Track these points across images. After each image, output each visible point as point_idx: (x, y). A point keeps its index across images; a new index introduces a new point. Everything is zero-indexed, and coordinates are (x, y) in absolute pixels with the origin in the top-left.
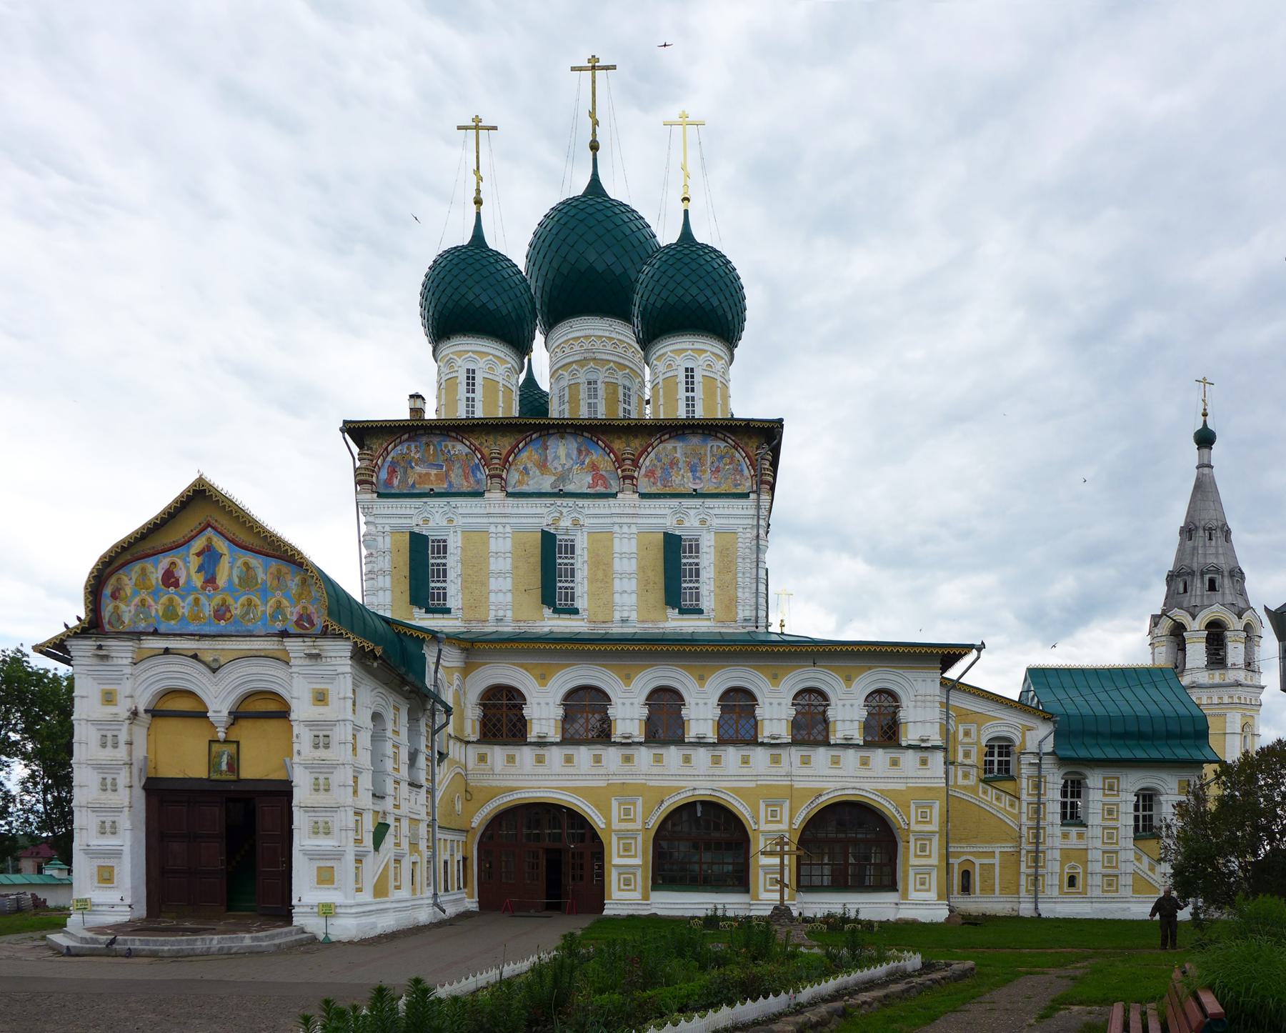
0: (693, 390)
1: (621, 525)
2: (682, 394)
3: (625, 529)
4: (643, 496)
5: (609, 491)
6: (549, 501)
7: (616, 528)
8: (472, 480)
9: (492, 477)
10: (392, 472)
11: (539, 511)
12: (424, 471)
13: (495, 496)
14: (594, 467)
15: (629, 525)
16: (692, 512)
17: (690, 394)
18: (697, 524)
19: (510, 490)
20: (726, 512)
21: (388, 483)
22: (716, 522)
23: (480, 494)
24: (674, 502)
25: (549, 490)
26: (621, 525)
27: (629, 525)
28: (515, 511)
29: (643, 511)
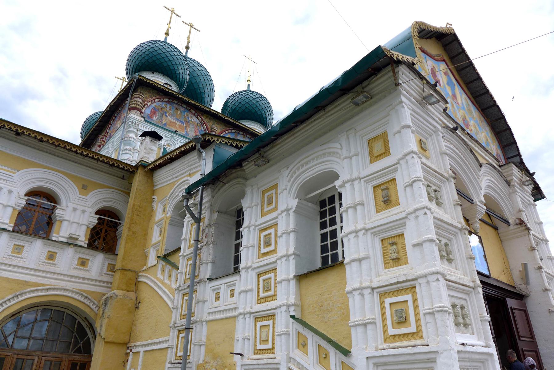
10: (154, 111)
12: (173, 121)
21: (150, 116)
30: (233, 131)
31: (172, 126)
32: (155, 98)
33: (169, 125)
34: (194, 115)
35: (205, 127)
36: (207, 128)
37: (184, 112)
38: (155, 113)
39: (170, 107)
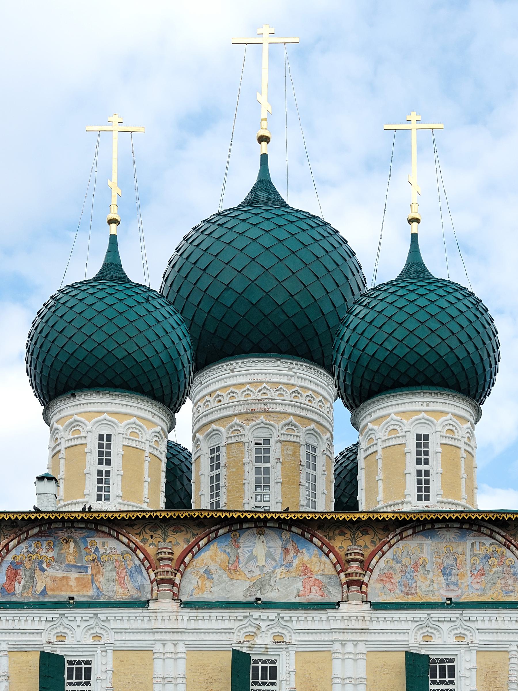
0: (427, 462)
1: (343, 643)
2: (412, 467)
3: (350, 648)
4: (376, 606)
5: (327, 600)
6: (240, 613)
7: (337, 646)
8: (129, 586)
9: (160, 582)
11: (226, 625)
12: (60, 574)
13: (165, 606)
14: (306, 570)
15: (355, 643)
16: (445, 626)
17: (423, 467)
18: (451, 640)
19: (184, 599)
20: (494, 625)
22: (479, 638)
23: (144, 604)
24: (421, 614)
25: (241, 598)
26: (343, 643)
27: (355, 643)
28: (193, 625)
29: (375, 626)
30: (221, 532)
31: (59, 589)
32: (4, 542)
33: (53, 590)
34: (109, 534)
35: (142, 556)
36: (146, 558)
37: (84, 539)
38: (16, 574)
39: (49, 544)
